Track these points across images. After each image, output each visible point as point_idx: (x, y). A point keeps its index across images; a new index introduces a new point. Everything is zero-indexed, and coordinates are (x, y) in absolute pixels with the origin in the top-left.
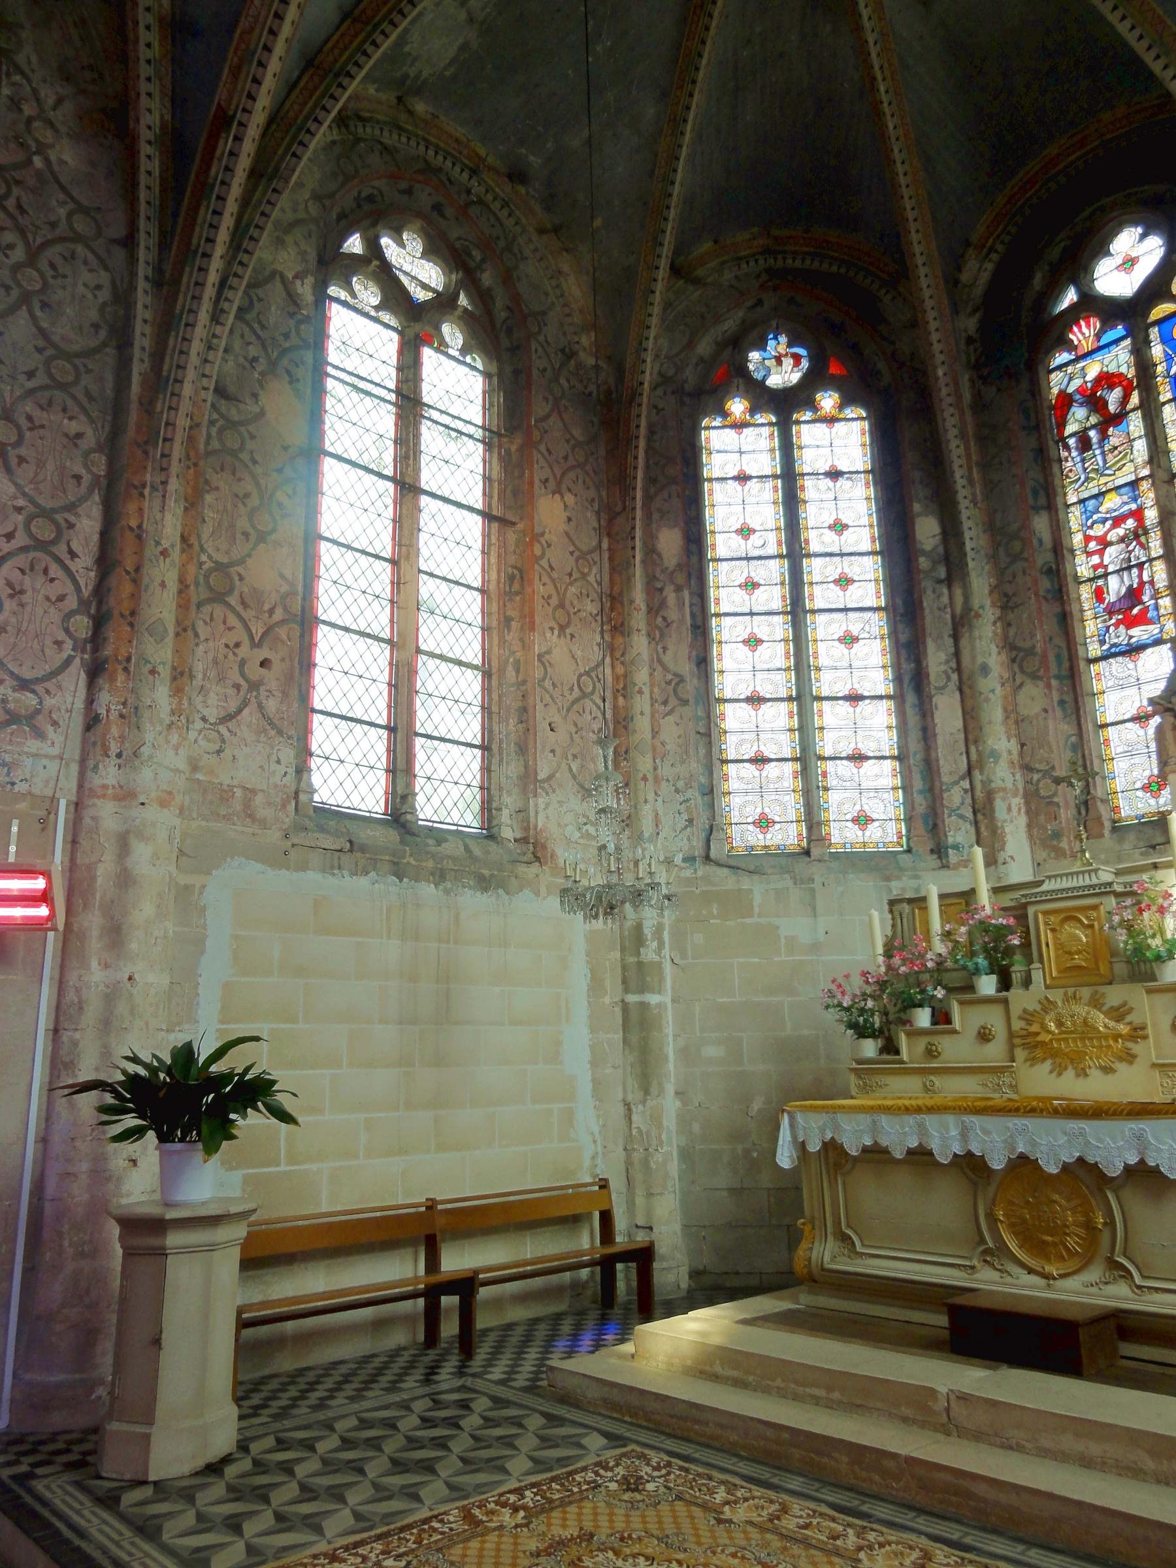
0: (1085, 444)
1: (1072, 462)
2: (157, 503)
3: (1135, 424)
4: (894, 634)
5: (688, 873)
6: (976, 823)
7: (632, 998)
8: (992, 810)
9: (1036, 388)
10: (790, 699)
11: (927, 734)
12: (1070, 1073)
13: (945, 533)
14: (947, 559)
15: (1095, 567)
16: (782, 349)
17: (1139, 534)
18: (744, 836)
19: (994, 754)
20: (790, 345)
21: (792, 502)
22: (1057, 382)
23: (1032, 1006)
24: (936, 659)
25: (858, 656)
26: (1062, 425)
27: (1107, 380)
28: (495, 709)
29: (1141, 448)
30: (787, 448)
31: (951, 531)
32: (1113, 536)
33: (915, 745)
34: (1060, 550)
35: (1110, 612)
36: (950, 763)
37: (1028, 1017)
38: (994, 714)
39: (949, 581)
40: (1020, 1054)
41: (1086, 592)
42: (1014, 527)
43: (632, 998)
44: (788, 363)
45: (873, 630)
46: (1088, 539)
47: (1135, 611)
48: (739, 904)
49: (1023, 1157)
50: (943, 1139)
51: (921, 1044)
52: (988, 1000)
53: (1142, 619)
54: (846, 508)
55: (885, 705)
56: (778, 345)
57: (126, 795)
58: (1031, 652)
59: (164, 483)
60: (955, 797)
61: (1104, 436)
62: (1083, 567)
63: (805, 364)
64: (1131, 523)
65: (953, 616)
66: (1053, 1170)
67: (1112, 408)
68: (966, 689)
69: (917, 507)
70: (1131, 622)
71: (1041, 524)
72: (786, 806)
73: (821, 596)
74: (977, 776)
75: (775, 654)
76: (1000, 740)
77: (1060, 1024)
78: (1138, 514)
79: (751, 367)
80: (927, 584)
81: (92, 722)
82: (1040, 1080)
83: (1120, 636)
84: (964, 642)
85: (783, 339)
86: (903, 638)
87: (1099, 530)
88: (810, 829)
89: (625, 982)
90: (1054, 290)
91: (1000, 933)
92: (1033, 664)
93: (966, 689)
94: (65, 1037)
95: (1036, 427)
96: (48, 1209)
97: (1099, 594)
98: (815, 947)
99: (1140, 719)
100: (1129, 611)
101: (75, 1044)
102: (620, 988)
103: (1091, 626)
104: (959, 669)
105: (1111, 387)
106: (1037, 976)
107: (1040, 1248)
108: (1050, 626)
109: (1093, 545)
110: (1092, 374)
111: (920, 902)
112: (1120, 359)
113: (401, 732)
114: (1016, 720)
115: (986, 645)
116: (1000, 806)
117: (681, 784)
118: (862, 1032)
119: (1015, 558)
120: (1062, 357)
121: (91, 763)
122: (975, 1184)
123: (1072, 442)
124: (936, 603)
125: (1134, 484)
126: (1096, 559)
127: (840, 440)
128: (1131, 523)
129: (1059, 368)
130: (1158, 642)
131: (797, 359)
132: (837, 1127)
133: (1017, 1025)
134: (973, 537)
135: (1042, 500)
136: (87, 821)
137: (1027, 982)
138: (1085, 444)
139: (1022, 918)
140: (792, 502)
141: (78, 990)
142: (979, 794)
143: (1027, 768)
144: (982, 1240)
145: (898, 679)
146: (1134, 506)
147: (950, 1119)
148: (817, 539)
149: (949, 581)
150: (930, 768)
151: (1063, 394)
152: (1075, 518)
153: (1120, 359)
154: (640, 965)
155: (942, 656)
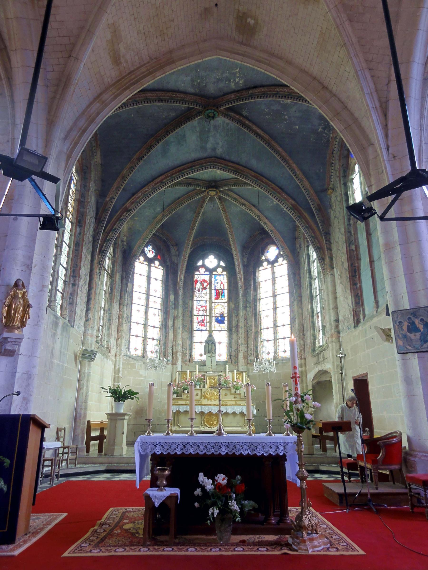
0: (199, 291)
1: (196, 293)
2: (99, 277)
3: (208, 290)
4: (162, 316)
5: (125, 358)
6: (173, 356)
7: (116, 384)
8: (177, 355)
9: (193, 277)
10: (143, 324)
11: (166, 337)
12: (210, 401)
13: (175, 299)
14: (175, 304)
15: (198, 314)
16: (151, 249)
17: (205, 310)
18: (132, 352)
19: (179, 344)
20: (152, 249)
21: (149, 283)
22: (196, 277)
23: (205, 391)
24: (170, 323)
25: (155, 319)
26: (196, 285)
27: (204, 281)
28: (105, 318)
29: (208, 296)
30: (149, 271)
32: (201, 309)
33: (163, 339)
34: (192, 309)
35: (199, 322)
36: (170, 344)
37: (204, 392)
38: (179, 336)
39: (174, 308)
40: (202, 398)
41: (195, 318)
42: (187, 302)
43: (116, 384)
44: (151, 252)
45: (158, 313)
46: (197, 308)
47: (203, 324)
48: (133, 366)
49: (210, 412)
50: (198, 410)
51: (186, 396)
52: (198, 389)
53: (204, 325)
54: (157, 287)
55: (159, 329)
56: (150, 248)
57: (92, 336)
58: (186, 326)
59: (100, 273)
60: (170, 351)
61: (202, 291)
62: (195, 313)
63: (154, 254)
64: (204, 308)
65: (174, 316)
66: (214, 413)
67: (205, 286)
69: (171, 292)
70: (202, 325)
71: (190, 302)
72: (140, 347)
73: (151, 304)
74: (175, 348)
75: (142, 314)
76: (180, 342)
77: (209, 394)
78: (206, 307)
79: (145, 251)
80: (171, 308)
81: (87, 320)
82: (205, 402)
83: (200, 327)
84: (176, 321)
85: (151, 247)
86: (164, 317)
87: (199, 307)
88: (144, 353)
89: (114, 380)
90: (198, 260)
91: (201, 379)
92: (186, 329)
94: (82, 382)
95: (192, 284)
96: (78, 415)
97: (197, 319)
98: (145, 377)
99: (201, 343)
100: (202, 323)
101: (83, 384)
102: (113, 381)
103: (195, 324)
104: (174, 326)
105: (205, 282)
106: (206, 386)
107: (210, 424)
108: (190, 321)
109: (198, 310)
110: (202, 279)
111: (185, 373)
112: (207, 278)
114: (183, 339)
115: (179, 323)
116: (178, 354)
117: (126, 339)
118: (174, 393)
119: (186, 308)
120: (197, 273)
121: (87, 328)
122: (202, 416)
123: (197, 289)
124: (172, 312)
125: (206, 301)
126: (198, 312)
127: (158, 272)
128: (204, 308)
129: (197, 274)
130: (206, 330)
131: (153, 252)
132: (179, 408)
133: (203, 393)
134: (181, 303)
135: (191, 298)
136: (86, 340)
137: (204, 387)
138: (199, 291)
139: (205, 377)
140: (149, 283)
141: (84, 373)
142: (174, 351)
143: (183, 348)
144: (202, 424)
145: (162, 325)
146: (205, 305)
147: (200, 406)
148: (152, 292)
149: (174, 308)
150: (166, 344)
151: (196, 280)
152: (195, 303)
153: (207, 278)
154: (118, 377)
155: (171, 323)
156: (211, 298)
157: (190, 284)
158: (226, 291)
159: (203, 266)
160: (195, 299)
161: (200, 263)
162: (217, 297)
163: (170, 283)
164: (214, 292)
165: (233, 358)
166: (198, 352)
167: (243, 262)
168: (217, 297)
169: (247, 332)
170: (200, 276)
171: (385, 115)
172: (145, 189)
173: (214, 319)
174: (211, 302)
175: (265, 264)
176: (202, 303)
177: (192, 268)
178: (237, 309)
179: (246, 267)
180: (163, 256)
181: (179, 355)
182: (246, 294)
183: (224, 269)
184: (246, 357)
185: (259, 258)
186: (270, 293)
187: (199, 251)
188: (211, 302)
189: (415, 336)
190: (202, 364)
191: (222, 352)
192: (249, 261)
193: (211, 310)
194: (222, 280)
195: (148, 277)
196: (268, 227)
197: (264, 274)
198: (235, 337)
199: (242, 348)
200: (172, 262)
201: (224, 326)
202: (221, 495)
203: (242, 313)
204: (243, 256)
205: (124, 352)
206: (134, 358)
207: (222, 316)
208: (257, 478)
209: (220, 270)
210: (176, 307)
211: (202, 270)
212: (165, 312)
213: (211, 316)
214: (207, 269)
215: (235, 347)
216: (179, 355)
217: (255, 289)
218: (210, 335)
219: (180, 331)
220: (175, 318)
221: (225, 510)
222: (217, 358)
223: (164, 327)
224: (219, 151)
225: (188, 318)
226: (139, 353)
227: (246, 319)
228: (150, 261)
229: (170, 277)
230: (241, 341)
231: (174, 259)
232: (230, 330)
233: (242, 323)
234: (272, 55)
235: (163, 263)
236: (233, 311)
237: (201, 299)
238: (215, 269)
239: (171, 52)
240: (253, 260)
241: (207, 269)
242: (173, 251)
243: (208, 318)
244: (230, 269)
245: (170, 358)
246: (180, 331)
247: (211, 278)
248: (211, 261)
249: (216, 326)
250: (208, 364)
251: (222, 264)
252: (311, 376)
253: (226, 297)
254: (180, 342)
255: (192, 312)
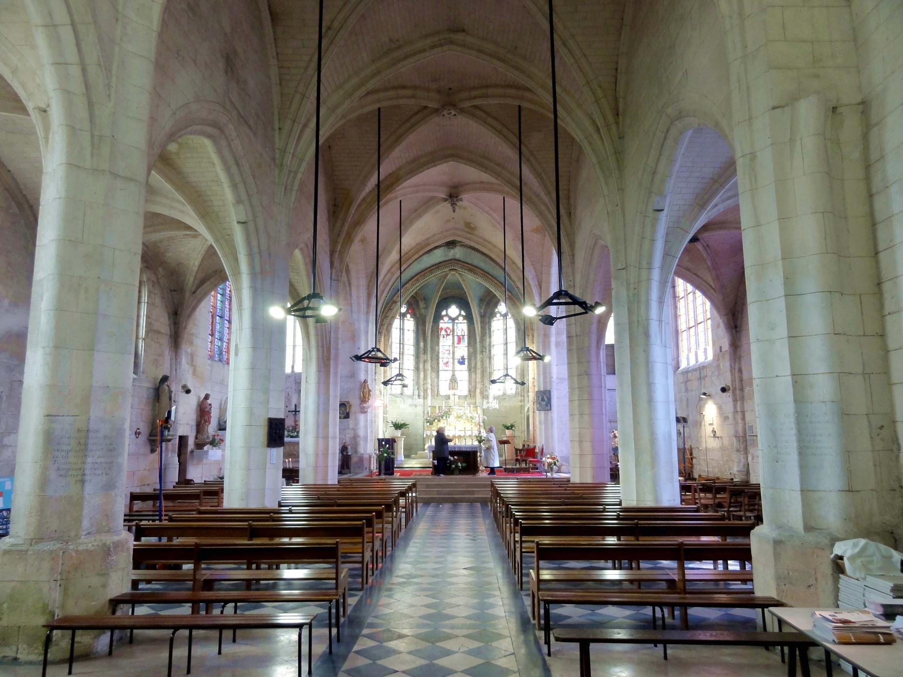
1: (441, 338)
3: (451, 337)
11: (418, 377)
24: (421, 366)
31: (425, 346)
36: (421, 382)
41: (440, 360)
48: (395, 402)
62: (441, 355)
68: (425, 371)
76: (429, 381)
93: (425, 371)
112: (450, 326)
113: (367, 371)
124: (422, 356)
127: (410, 324)
156: (453, 343)
157: (436, 331)
158: (466, 337)
159: (447, 315)
160: (441, 344)
161: (444, 313)
162: (459, 342)
163: (420, 332)
164: (456, 338)
165: (472, 393)
166: (444, 389)
167: (480, 313)
168: (459, 342)
169: (483, 372)
170: (444, 324)
171: (541, 288)
172: (407, 286)
173: (456, 361)
174: (454, 347)
175: (498, 315)
176: (447, 348)
177: (438, 317)
178: (475, 352)
179: (482, 316)
180: (413, 310)
181: (429, 392)
182: (482, 340)
183: (465, 318)
184: (482, 393)
185: (493, 310)
186: (502, 341)
187: (444, 303)
188: (454, 347)
189: (543, 403)
190: (448, 397)
191: (463, 388)
192: (485, 313)
193: (453, 353)
194: (462, 327)
195: (403, 331)
196: (497, 294)
197: (497, 324)
198: (473, 376)
199: (479, 386)
200: (421, 315)
201: (465, 367)
202: (455, 462)
203: (479, 357)
204: (480, 307)
205: (389, 392)
206: (395, 396)
207: (463, 358)
208: (468, 460)
209: (461, 318)
210: (425, 352)
211: (446, 319)
212: (417, 357)
213: (453, 358)
214: (450, 318)
215: (473, 384)
216: (429, 392)
217: (490, 337)
218: (453, 375)
219: (429, 372)
220: (425, 362)
221: (457, 466)
222: (458, 393)
223: (417, 368)
224: (457, 256)
225: (435, 361)
226: (399, 392)
227: (482, 362)
228: (403, 316)
229: (420, 328)
230: (479, 380)
231: (423, 311)
232: (470, 370)
233: (479, 364)
234: (485, 240)
235: (414, 315)
236: (472, 355)
237: (445, 343)
238: (457, 318)
239: (428, 239)
240: (488, 315)
241: (450, 318)
242: (422, 304)
243: (451, 360)
244: (469, 318)
245: (422, 394)
246: (429, 372)
247: (453, 326)
248: (453, 311)
249: (458, 366)
250: (452, 397)
251: (463, 313)
252: (526, 409)
253: (466, 342)
254: (429, 381)
255: (438, 356)
